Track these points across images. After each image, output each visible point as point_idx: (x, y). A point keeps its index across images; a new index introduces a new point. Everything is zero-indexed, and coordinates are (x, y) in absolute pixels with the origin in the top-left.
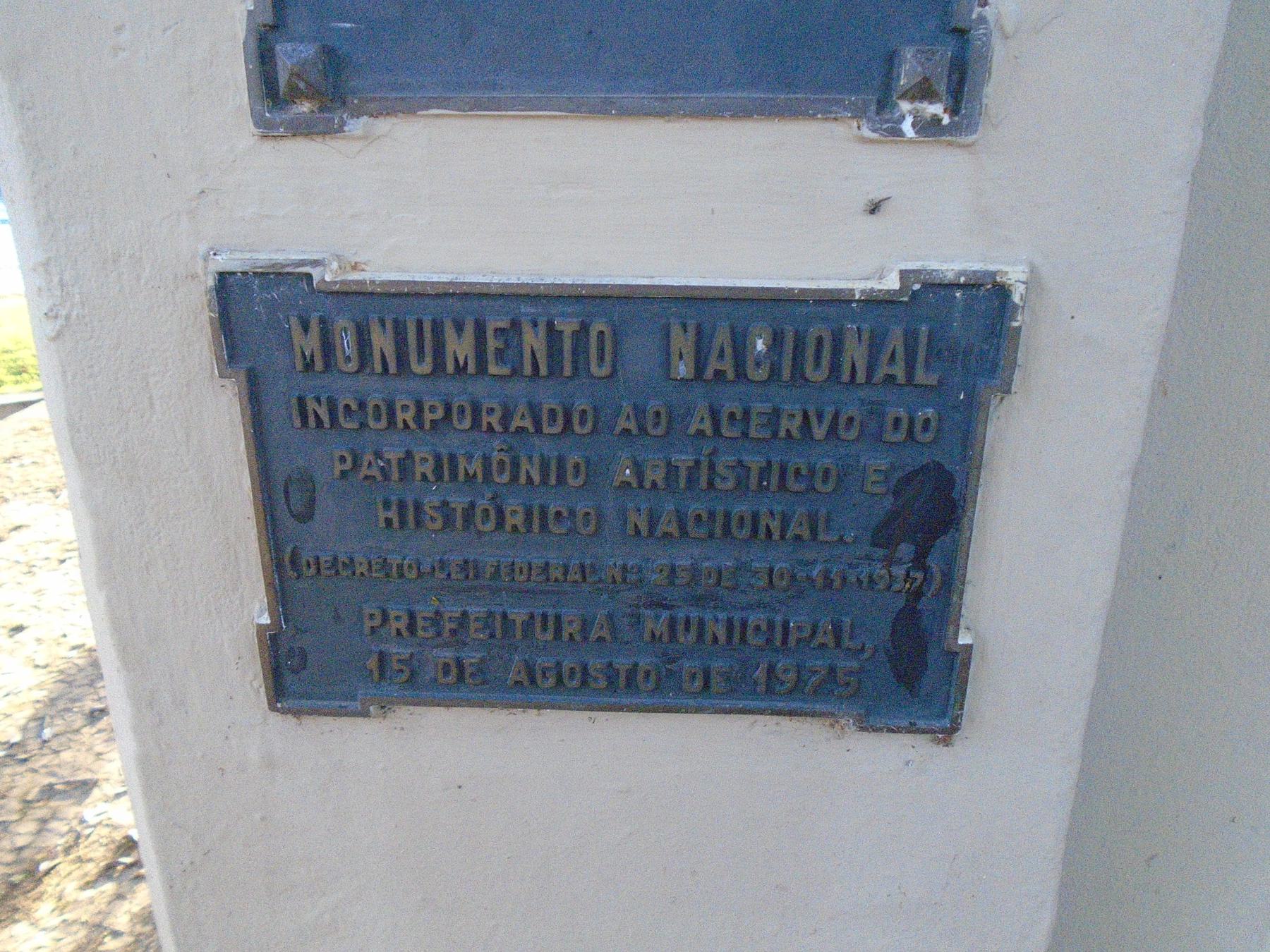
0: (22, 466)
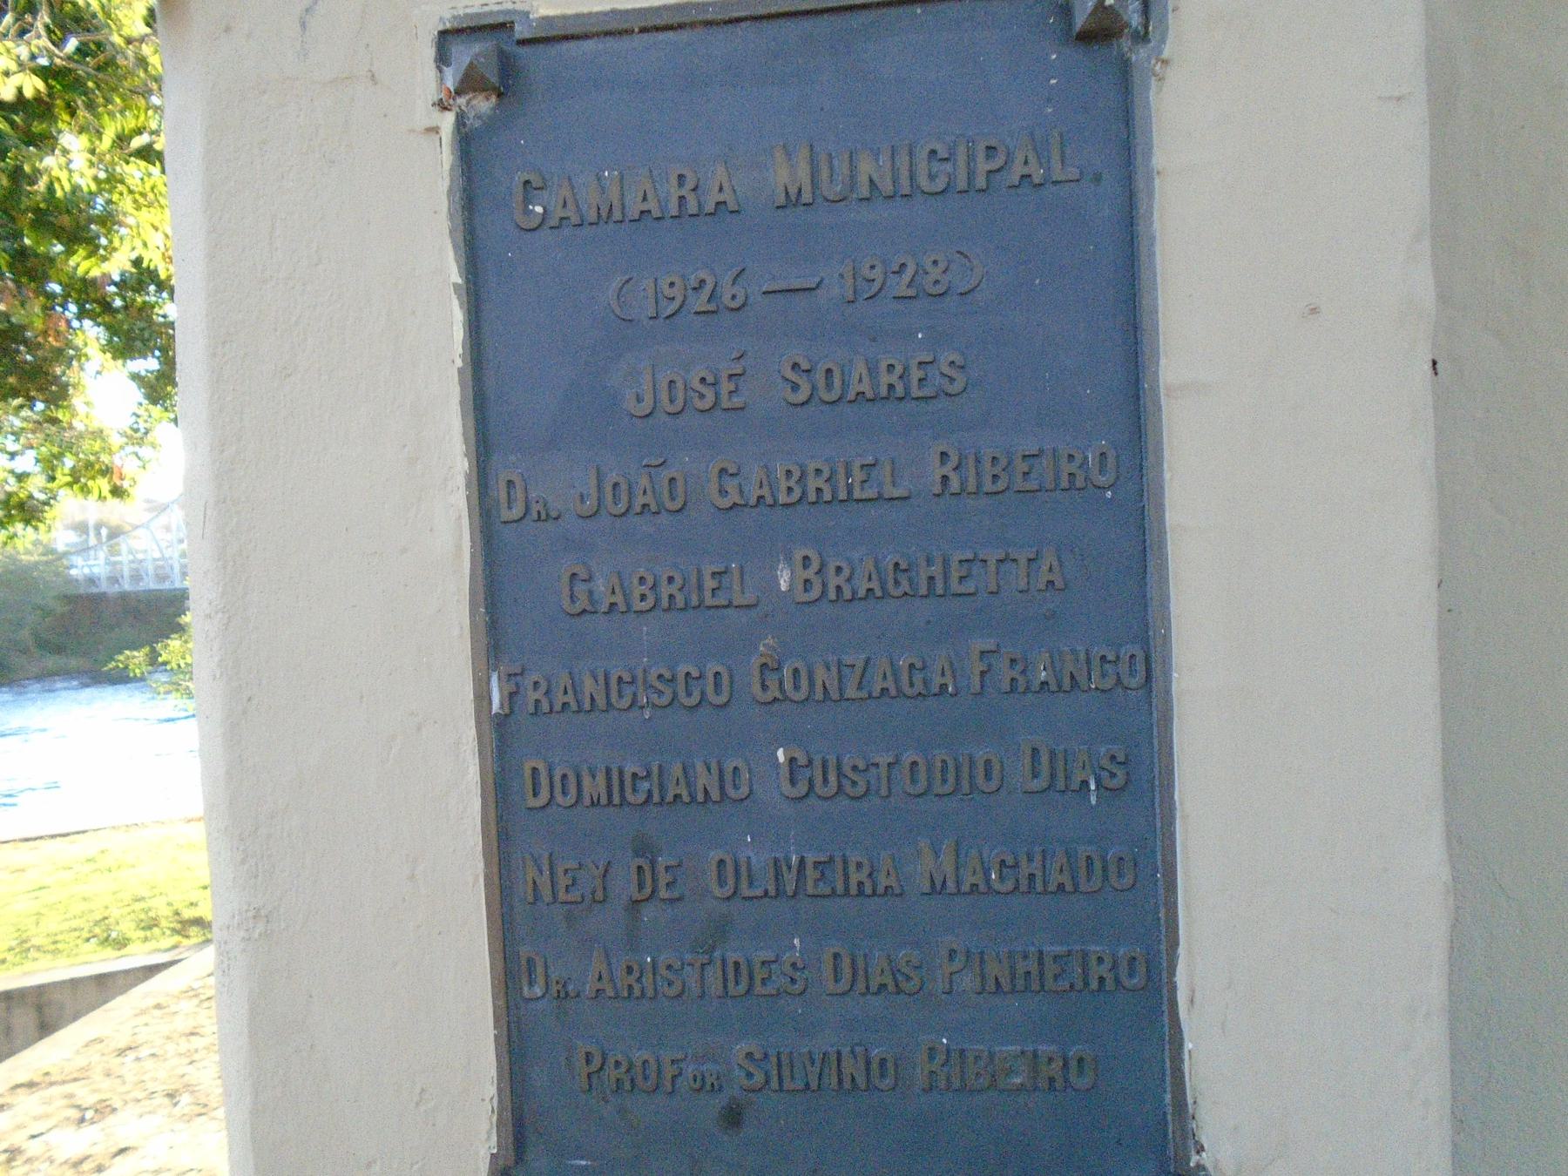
0: (138, 1059)
